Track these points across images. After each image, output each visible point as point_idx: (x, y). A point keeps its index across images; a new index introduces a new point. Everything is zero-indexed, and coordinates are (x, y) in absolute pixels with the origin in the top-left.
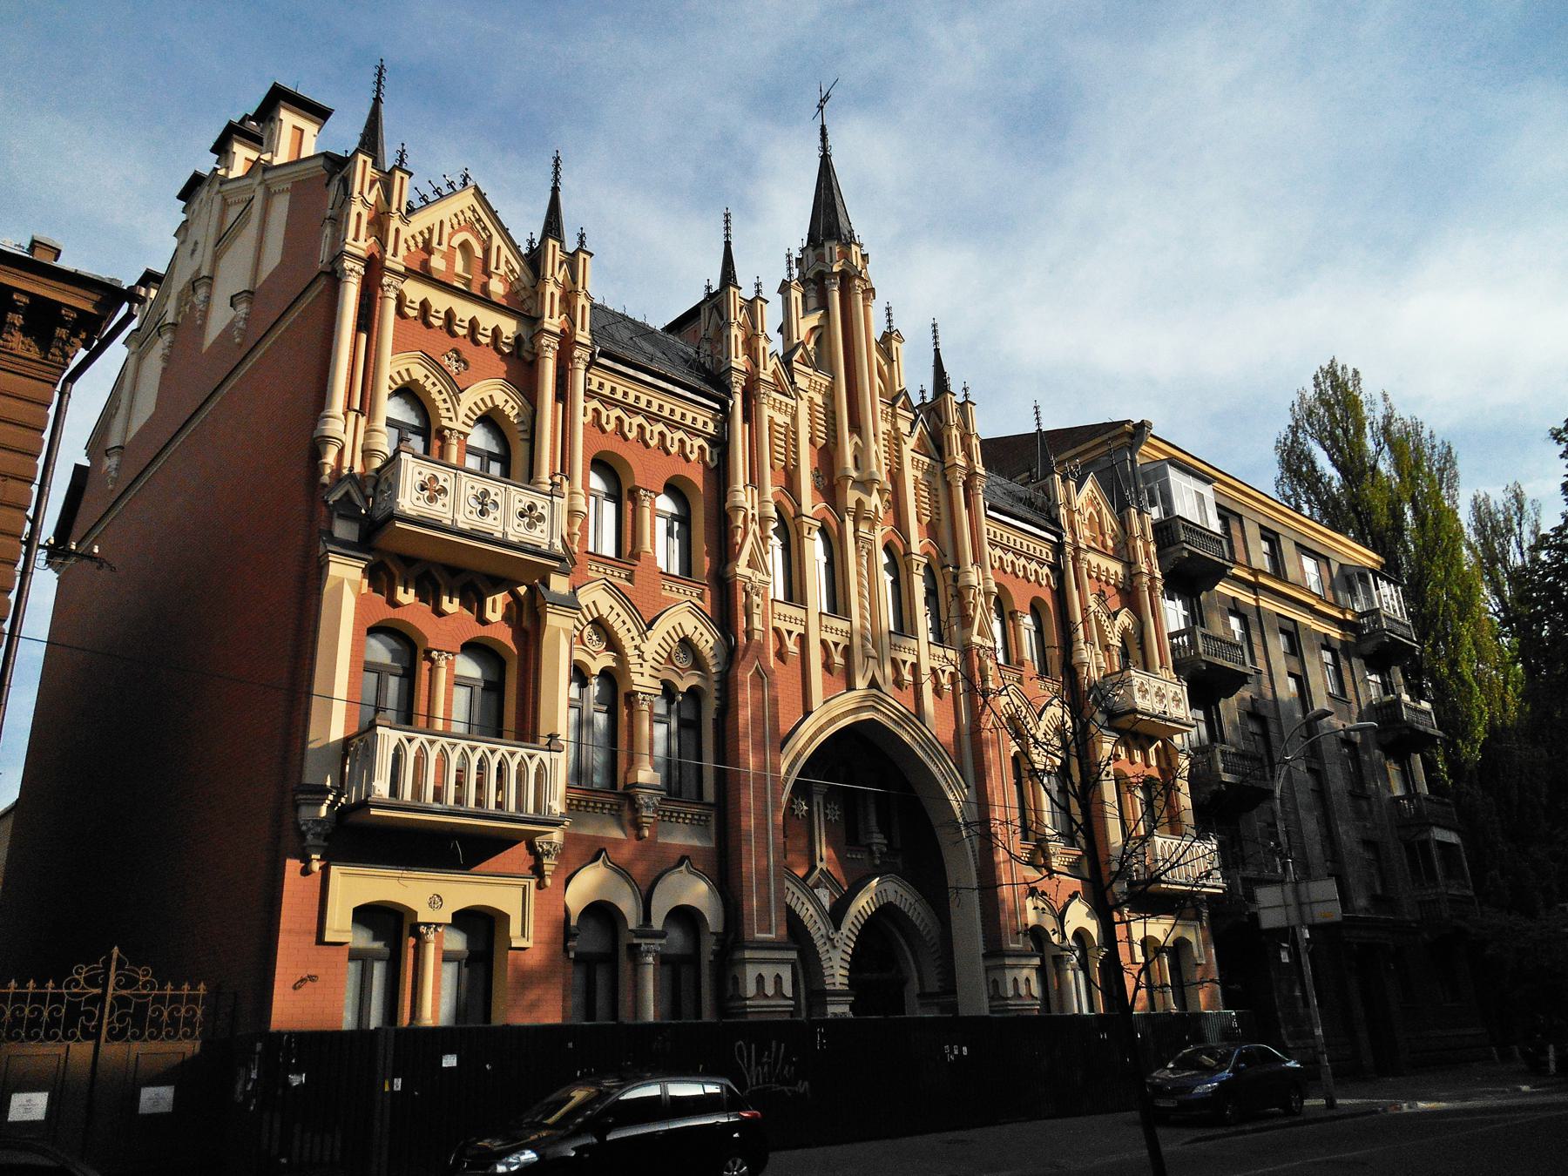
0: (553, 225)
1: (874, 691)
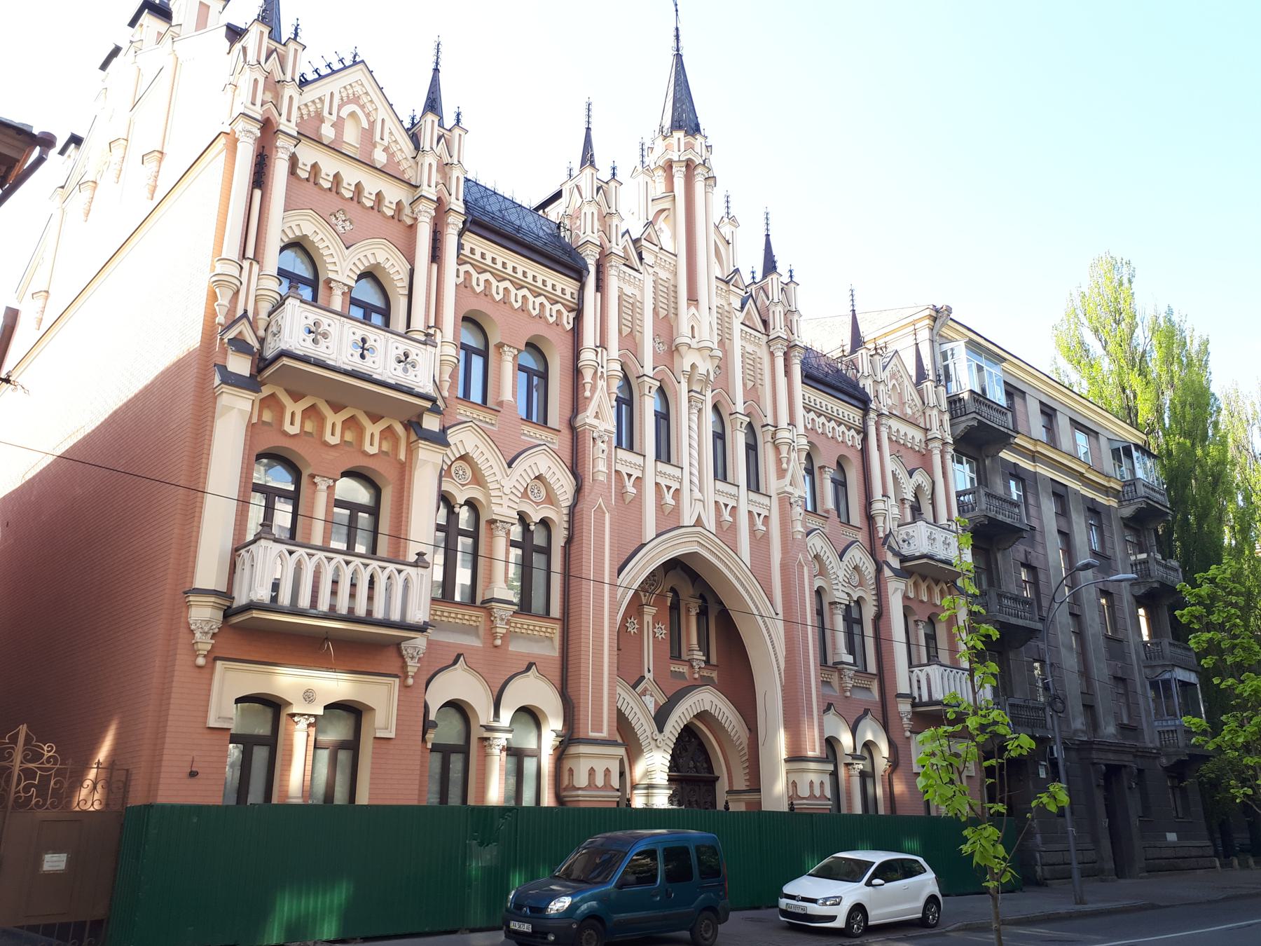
0: (433, 104)
1: (699, 529)
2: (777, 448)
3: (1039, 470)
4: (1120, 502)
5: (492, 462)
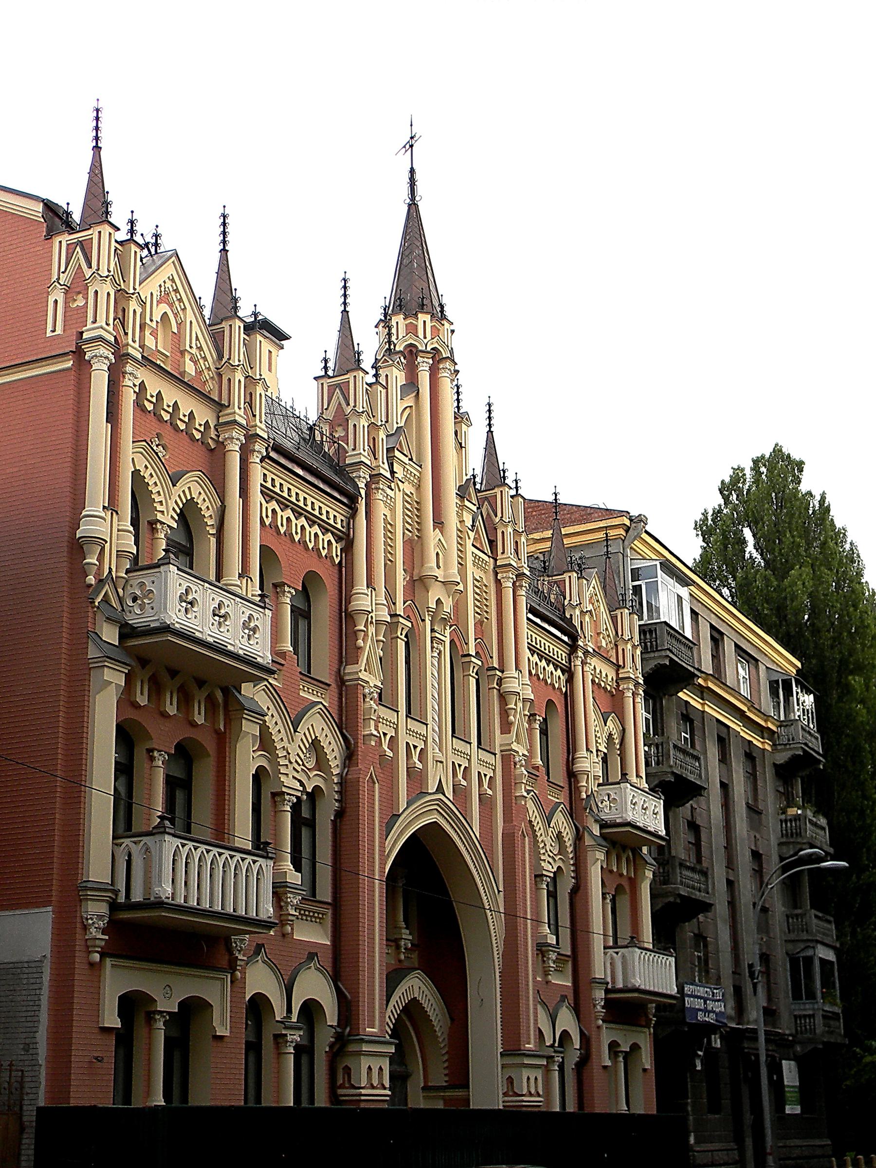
1: (441, 796)
2: (503, 698)
3: (707, 709)
4: (774, 745)
5: (280, 726)
